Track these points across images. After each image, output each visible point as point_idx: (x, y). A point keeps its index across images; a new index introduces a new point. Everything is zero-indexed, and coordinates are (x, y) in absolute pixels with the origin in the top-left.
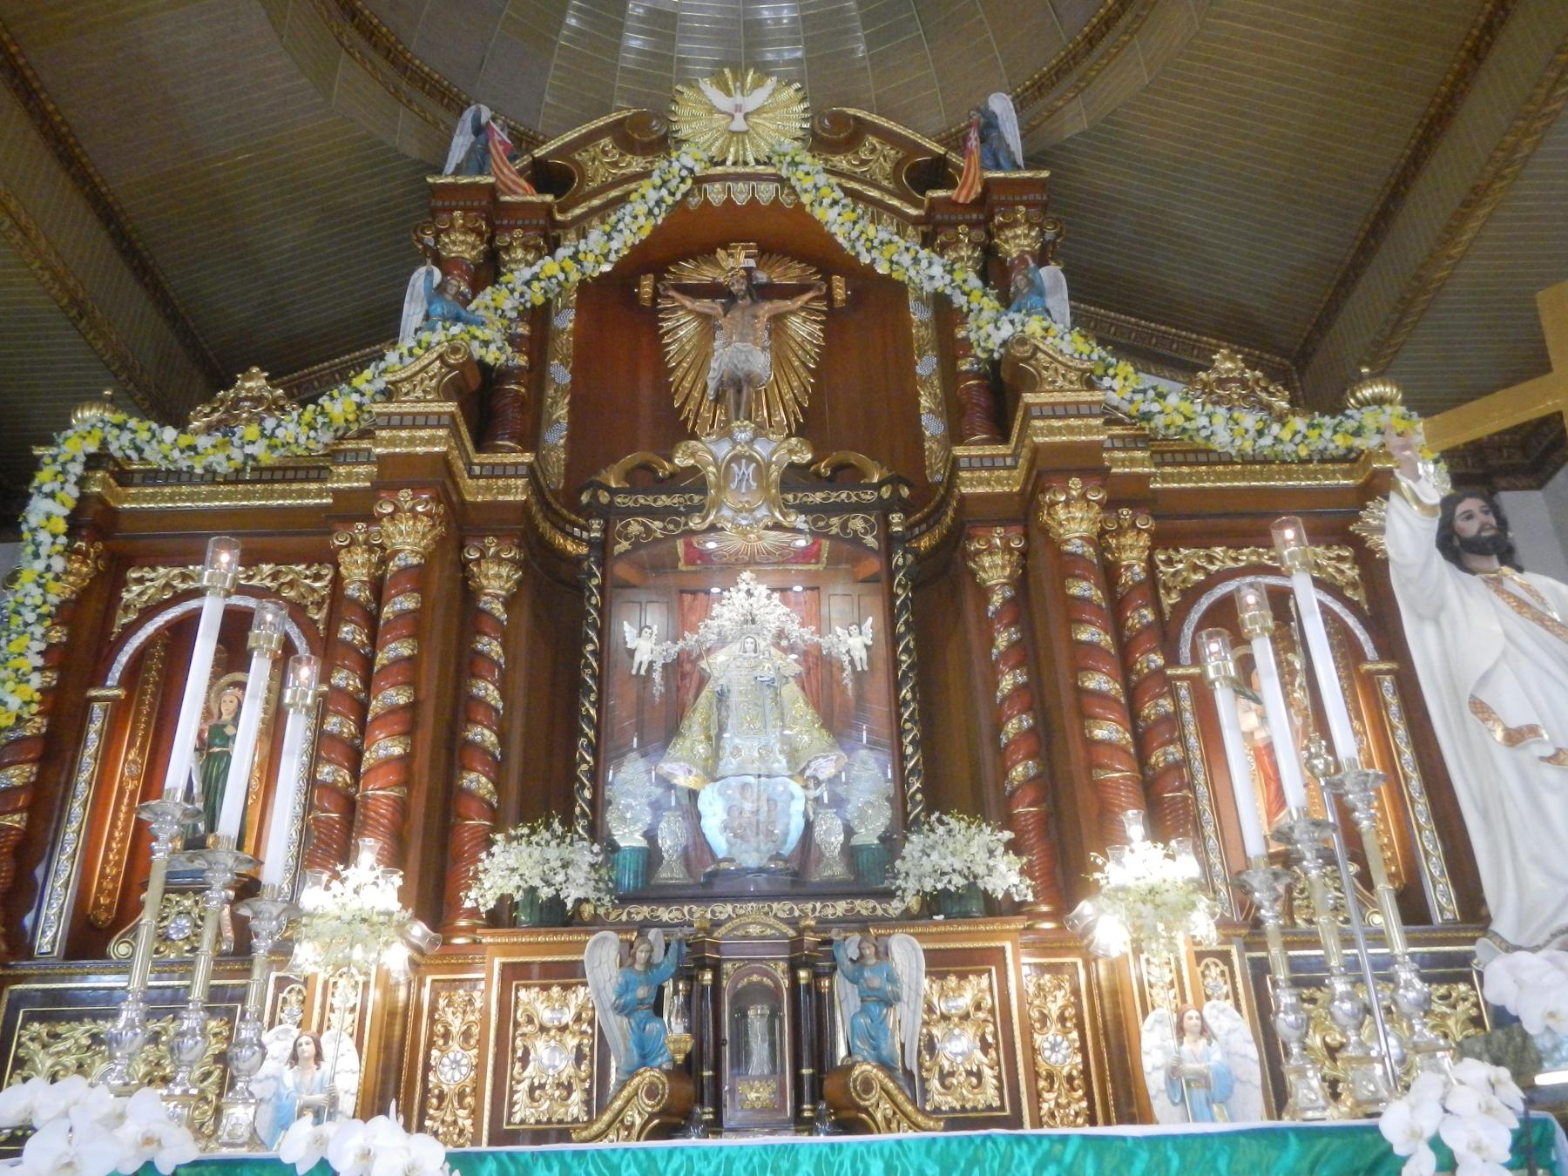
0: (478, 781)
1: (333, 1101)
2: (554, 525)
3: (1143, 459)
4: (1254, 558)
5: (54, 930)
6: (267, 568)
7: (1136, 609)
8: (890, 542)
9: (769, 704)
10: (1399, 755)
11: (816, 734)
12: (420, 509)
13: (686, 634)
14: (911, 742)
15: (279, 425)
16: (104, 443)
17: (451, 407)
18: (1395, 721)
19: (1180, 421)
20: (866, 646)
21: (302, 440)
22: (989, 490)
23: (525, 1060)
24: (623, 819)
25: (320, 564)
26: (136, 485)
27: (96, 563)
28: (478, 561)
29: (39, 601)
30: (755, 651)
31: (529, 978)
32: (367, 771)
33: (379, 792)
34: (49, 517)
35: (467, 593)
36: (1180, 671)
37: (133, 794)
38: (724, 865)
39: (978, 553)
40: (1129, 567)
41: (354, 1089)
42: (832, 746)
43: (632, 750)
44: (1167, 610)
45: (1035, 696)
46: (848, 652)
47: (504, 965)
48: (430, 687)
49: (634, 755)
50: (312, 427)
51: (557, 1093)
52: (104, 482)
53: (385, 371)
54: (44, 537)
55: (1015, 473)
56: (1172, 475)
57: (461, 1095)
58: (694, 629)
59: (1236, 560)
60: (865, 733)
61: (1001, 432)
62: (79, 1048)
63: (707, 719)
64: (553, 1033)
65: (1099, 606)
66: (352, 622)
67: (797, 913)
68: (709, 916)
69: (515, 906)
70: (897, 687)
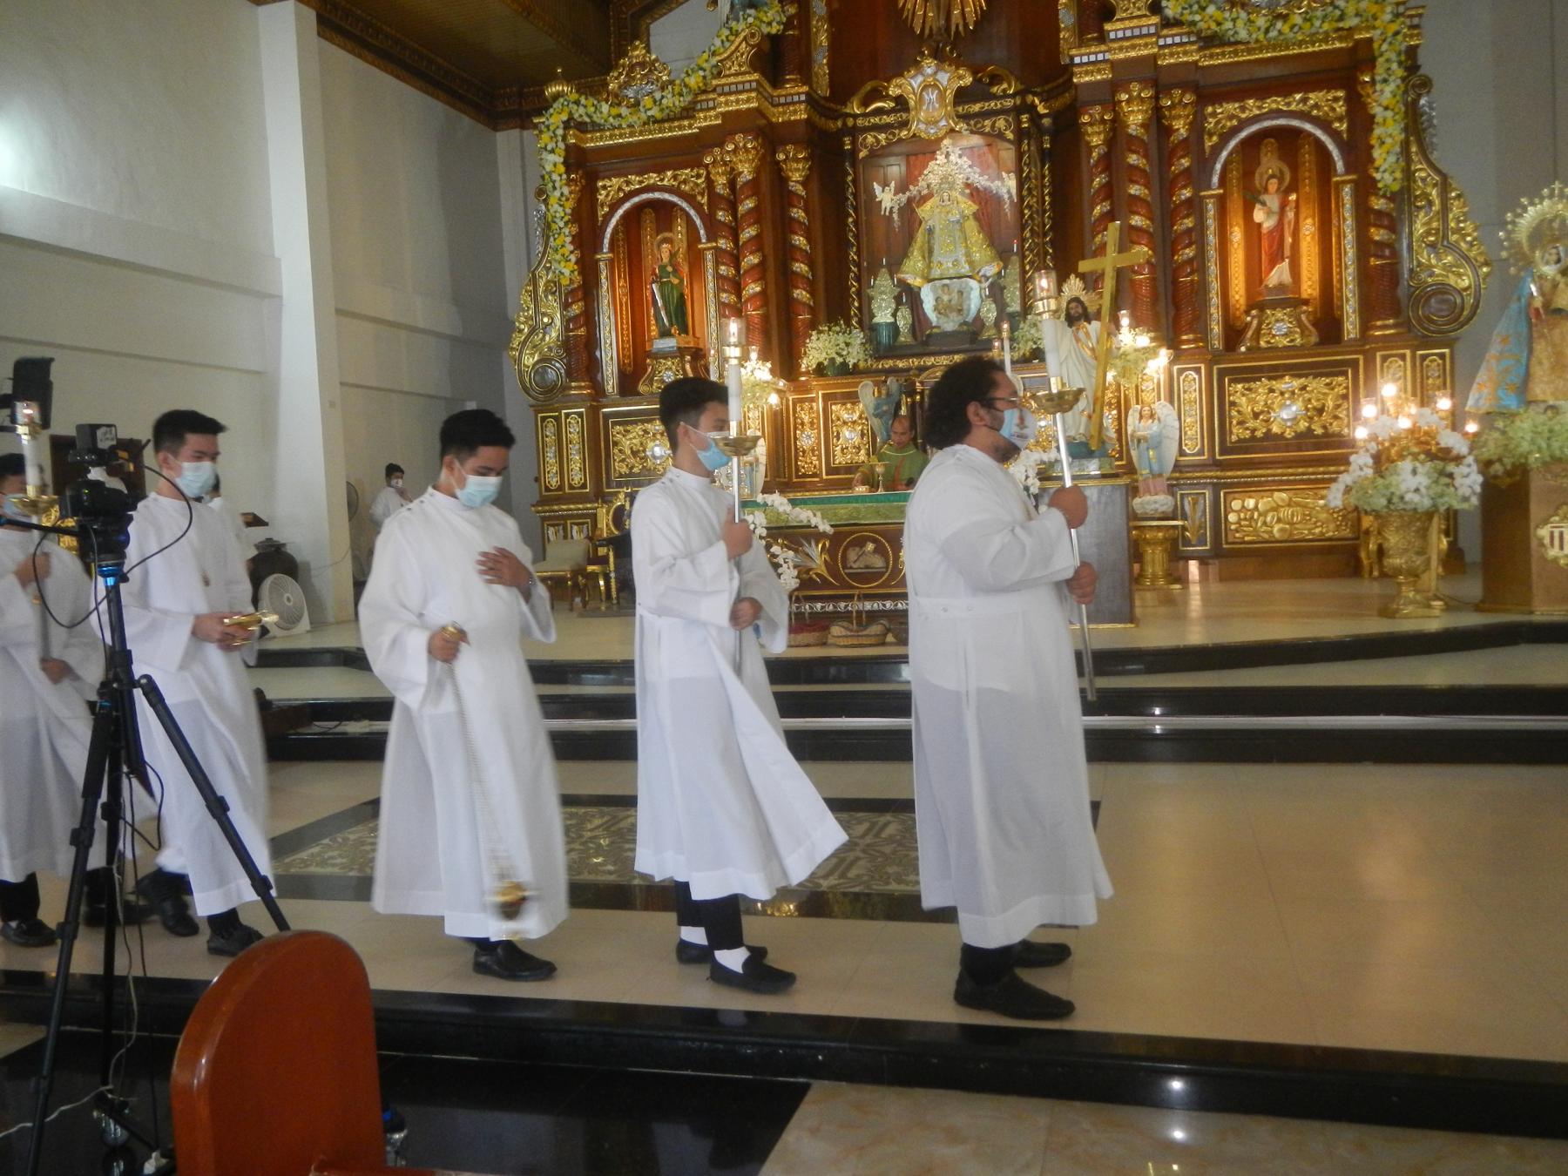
2: (828, 117)
4: (1274, 106)
6: (669, 173)
9: (958, 234)
10: (1345, 237)
12: (749, 146)
13: (911, 187)
15: (663, 97)
16: (570, 113)
17: (756, 76)
18: (1347, 215)
19: (1213, 26)
21: (677, 103)
22: (1093, 78)
24: (880, 307)
26: (590, 132)
28: (785, 161)
32: (746, 301)
34: (555, 165)
35: (780, 180)
37: (626, 303)
38: (935, 330)
40: (1178, 129)
41: (765, 452)
42: (991, 258)
43: (882, 266)
44: (1207, 150)
46: (1009, 192)
47: (824, 395)
48: (769, 249)
50: (681, 95)
52: (574, 135)
53: (714, 54)
54: (555, 177)
56: (1218, 54)
57: (813, 450)
59: (1260, 108)
61: (1103, 38)
63: (921, 247)
65: (1144, 171)
66: (722, 209)
69: (825, 368)
70: (1023, 229)
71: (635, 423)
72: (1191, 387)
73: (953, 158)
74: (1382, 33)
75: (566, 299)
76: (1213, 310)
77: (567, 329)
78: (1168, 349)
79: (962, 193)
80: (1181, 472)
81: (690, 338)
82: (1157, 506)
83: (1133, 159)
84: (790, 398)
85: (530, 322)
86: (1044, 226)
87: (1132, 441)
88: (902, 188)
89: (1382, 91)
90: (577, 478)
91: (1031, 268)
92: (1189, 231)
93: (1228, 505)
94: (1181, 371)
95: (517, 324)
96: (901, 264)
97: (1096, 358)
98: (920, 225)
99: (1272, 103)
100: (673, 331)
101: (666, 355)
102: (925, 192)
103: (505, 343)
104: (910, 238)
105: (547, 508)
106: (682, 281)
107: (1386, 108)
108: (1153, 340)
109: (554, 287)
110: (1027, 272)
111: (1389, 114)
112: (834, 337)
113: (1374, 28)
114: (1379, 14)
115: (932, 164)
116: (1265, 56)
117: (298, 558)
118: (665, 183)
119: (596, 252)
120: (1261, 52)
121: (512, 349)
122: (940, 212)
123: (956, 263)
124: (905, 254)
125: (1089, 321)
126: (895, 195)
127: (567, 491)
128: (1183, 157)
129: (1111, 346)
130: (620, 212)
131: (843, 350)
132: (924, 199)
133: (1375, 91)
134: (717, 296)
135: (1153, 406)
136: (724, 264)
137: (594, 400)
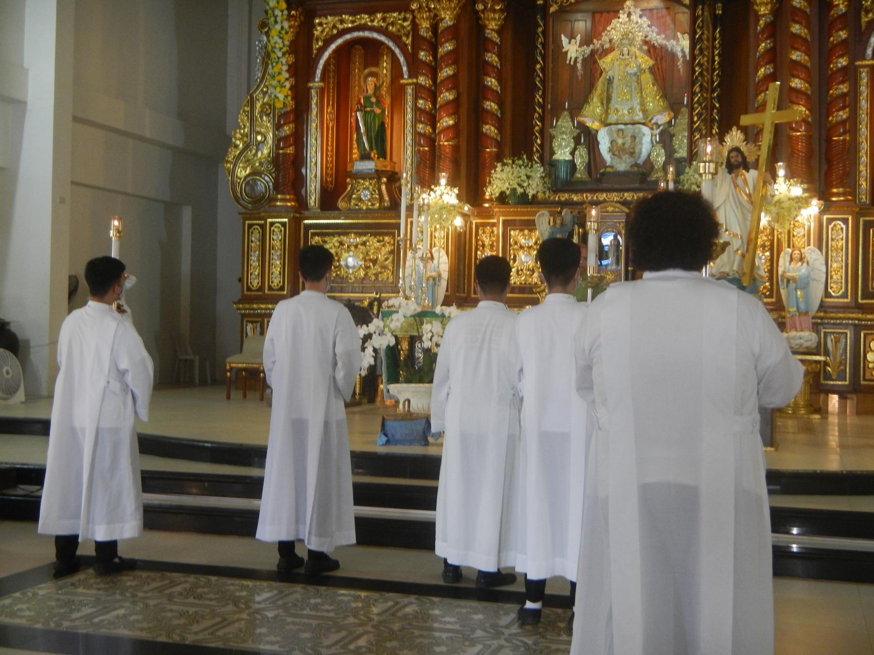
0: (490, 130)
1: (440, 275)
5: (314, 196)
6: (379, 16)
7: (837, 31)
9: (634, 84)
11: (656, 102)
13: (595, 41)
14: (697, 114)
23: (515, 260)
24: (560, 146)
27: (300, 18)
28: (483, 11)
29: (281, 45)
31: (515, 226)
32: (440, 133)
33: (446, 143)
35: (480, 28)
38: (608, 170)
40: (838, 5)
43: (564, 109)
44: (864, 25)
46: (682, 51)
47: (504, 222)
49: (566, 113)
51: (528, 273)
54: (277, 12)
58: (599, 36)
60: (686, 99)
62: (335, 246)
63: (601, 95)
64: (526, 249)
65: (805, 40)
66: (423, 50)
67: (635, 198)
68: (595, 198)
69: (507, 197)
70: (693, 84)
71: (333, 235)
72: (838, 235)
73: (634, 17)
75: (279, 120)
76: (862, 168)
77: (278, 147)
78: (819, 199)
79: (638, 49)
80: (825, 312)
82: (802, 341)
83: (796, 28)
84: (474, 222)
85: (245, 139)
86: (713, 82)
87: (782, 281)
88: (587, 41)
90: (276, 281)
91: (698, 119)
92: (844, 95)
93: (867, 345)
94: (830, 221)
95: (234, 140)
96: (582, 108)
97: (752, 203)
98: (601, 76)
100: (372, 155)
101: (364, 176)
102: (607, 46)
103: (222, 157)
104: (591, 86)
105: (247, 306)
106: (383, 112)
108: (805, 190)
109: (269, 109)
110: (695, 123)
112: (516, 170)
115: (614, 21)
117: (20, 336)
118: (375, 23)
119: (309, 81)
121: (227, 162)
122: (620, 65)
123: (631, 110)
124: (585, 100)
125: (747, 169)
126: (580, 46)
127: (266, 291)
128: (842, 29)
129: (766, 193)
130: (333, 47)
131: (524, 181)
132: (606, 52)
134: (414, 126)
135: (803, 251)
136: (422, 98)
137: (296, 212)
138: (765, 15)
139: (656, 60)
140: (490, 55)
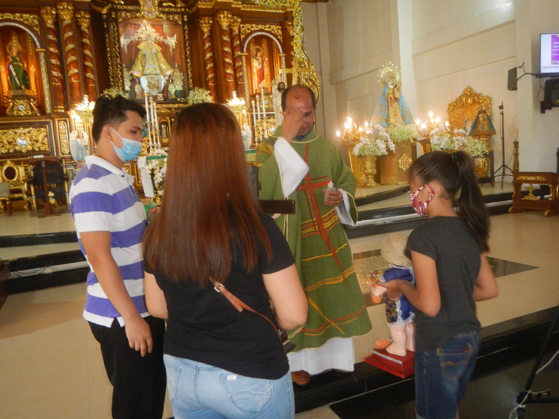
3: (240, 4)
4: (261, 28)
7: (236, 41)
8: (183, 21)
9: (155, 58)
12: (69, 8)
13: (132, 37)
20: (175, 42)
25: (34, 14)
28: (80, 18)
30: (151, 44)
32: (71, 76)
36: (243, 54)
39: (202, 23)
44: (242, 39)
45: (213, 59)
55: (211, 3)
59: (257, 28)
66: (50, 34)
70: (187, 58)
74: (296, 10)
81: (31, 92)
89: (296, 29)
99: (260, 27)
106: (24, 66)
107: (297, 34)
110: (189, 75)
111: (298, 36)
113: (293, 8)
114: (295, 4)
116: (259, 10)
118: (16, 19)
120: (259, 9)
123: (155, 69)
132: (138, 43)
133: (292, 29)
138: (207, 32)
139: (161, 47)
140: (85, 39)
